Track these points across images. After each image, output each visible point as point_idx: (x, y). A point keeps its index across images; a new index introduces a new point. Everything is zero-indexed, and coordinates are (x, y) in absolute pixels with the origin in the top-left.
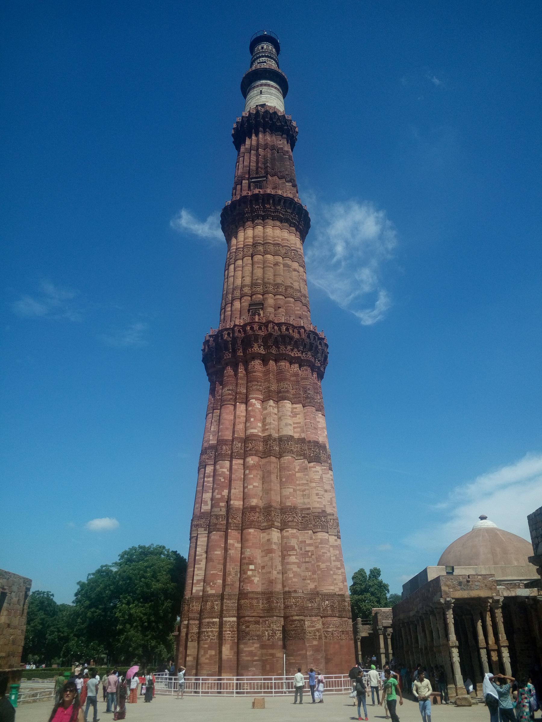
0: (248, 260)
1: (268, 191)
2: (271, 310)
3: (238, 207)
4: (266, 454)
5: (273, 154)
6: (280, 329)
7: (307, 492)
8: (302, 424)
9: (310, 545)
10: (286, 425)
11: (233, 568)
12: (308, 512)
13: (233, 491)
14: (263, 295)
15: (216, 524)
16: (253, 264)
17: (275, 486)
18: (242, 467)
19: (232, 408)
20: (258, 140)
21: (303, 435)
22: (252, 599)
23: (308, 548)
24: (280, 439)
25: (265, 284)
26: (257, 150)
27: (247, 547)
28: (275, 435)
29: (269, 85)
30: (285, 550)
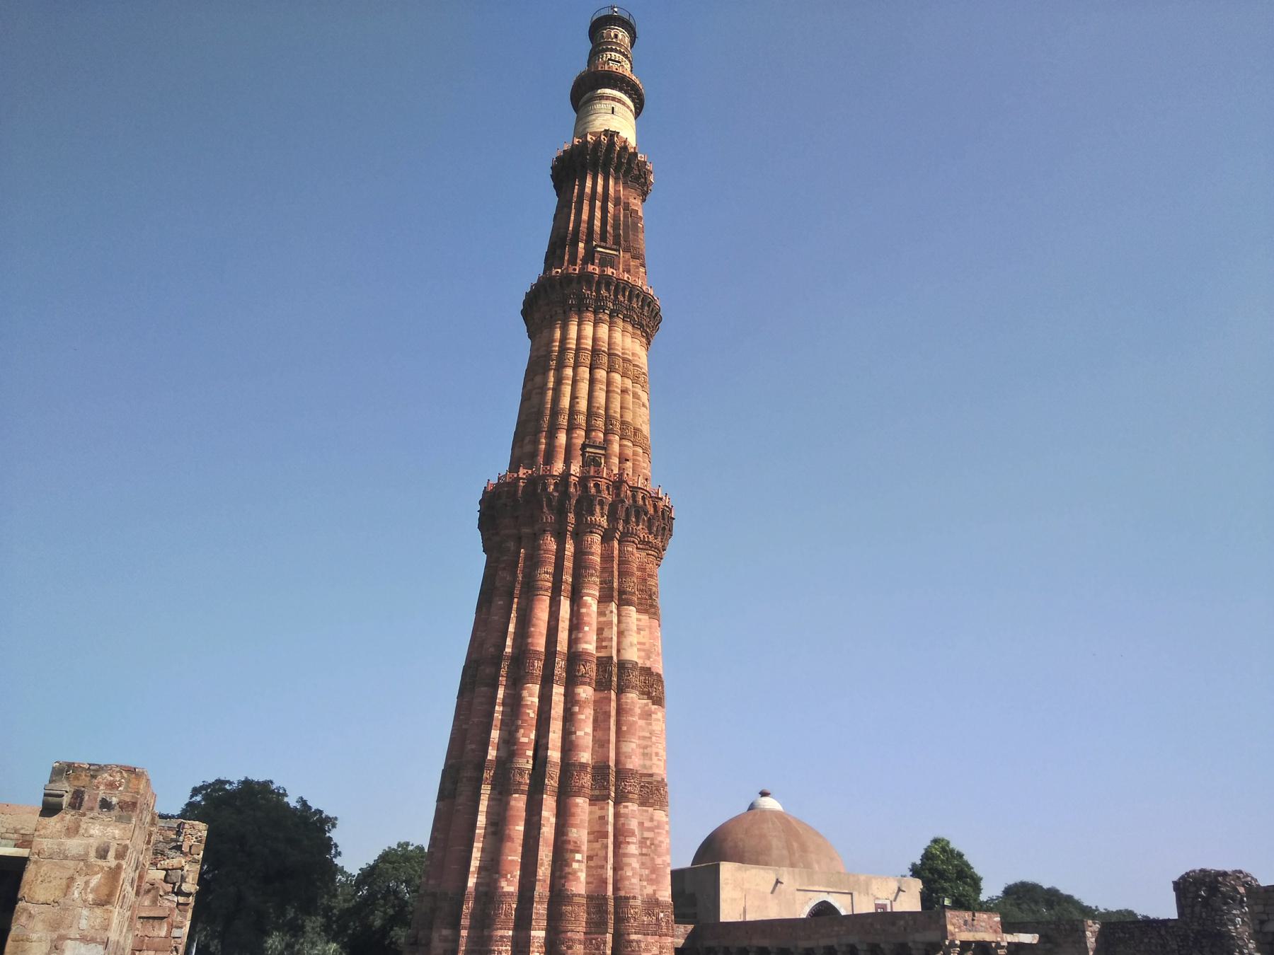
0: (584, 372)
2: (616, 460)
3: (574, 285)
5: (625, 216)
6: (634, 497)
7: (648, 750)
9: (650, 829)
10: (632, 645)
11: (545, 854)
12: (649, 779)
14: (605, 434)
15: (520, 783)
16: (592, 381)
18: (562, 698)
20: (606, 187)
22: (579, 905)
23: (647, 834)
24: (622, 665)
25: (608, 418)
27: (572, 826)
29: (624, 104)
30: (621, 835)
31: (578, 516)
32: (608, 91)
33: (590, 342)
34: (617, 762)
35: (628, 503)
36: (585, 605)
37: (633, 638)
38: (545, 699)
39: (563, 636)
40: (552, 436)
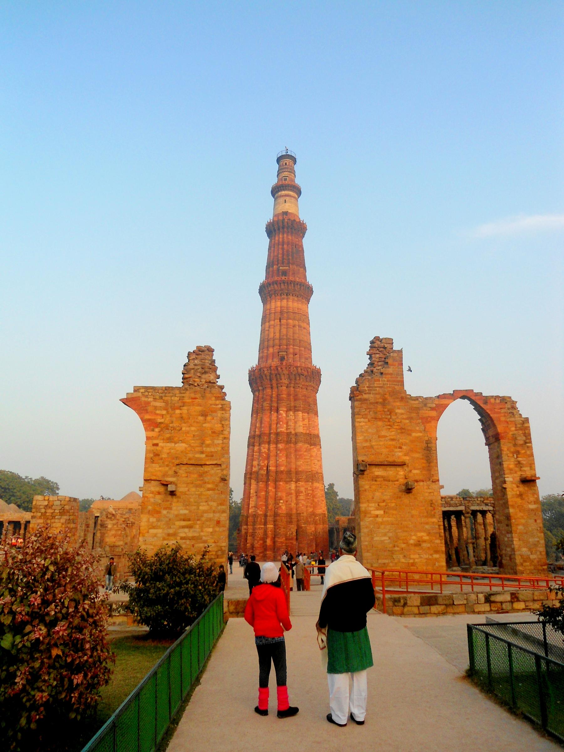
0: (277, 321)
1: (291, 278)
2: (292, 356)
3: (272, 286)
4: (288, 442)
5: (292, 248)
7: (309, 463)
8: (307, 425)
13: (271, 462)
16: (280, 325)
17: (293, 460)
19: (269, 414)
20: (283, 238)
21: (308, 432)
24: (296, 434)
25: (288, 339)
26: (283, 245)
28: (293, 432)
31: (277, 380)
32: (283, 193)
33: (279, 309)
34: (296, 469)
35: (294, 373)
36: (281, 414)
37: (301, 424)
38: (269, 449)
39: (274, 426)
40: (268, 350)
